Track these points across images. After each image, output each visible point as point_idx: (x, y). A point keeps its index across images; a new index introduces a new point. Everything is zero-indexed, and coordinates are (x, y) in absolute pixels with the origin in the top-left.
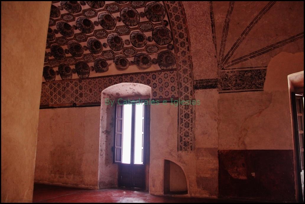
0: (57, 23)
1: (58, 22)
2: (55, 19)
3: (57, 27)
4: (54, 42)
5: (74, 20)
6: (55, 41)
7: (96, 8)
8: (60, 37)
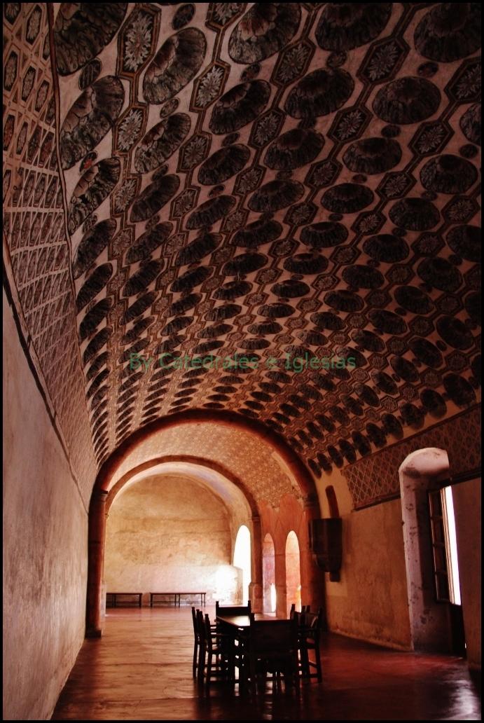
0: (447, 238)
1: (446, 233)
2: (435, 229)
3: (450, 247)
4: (464, 288)
6: (464, 285)
8: (471, 270)
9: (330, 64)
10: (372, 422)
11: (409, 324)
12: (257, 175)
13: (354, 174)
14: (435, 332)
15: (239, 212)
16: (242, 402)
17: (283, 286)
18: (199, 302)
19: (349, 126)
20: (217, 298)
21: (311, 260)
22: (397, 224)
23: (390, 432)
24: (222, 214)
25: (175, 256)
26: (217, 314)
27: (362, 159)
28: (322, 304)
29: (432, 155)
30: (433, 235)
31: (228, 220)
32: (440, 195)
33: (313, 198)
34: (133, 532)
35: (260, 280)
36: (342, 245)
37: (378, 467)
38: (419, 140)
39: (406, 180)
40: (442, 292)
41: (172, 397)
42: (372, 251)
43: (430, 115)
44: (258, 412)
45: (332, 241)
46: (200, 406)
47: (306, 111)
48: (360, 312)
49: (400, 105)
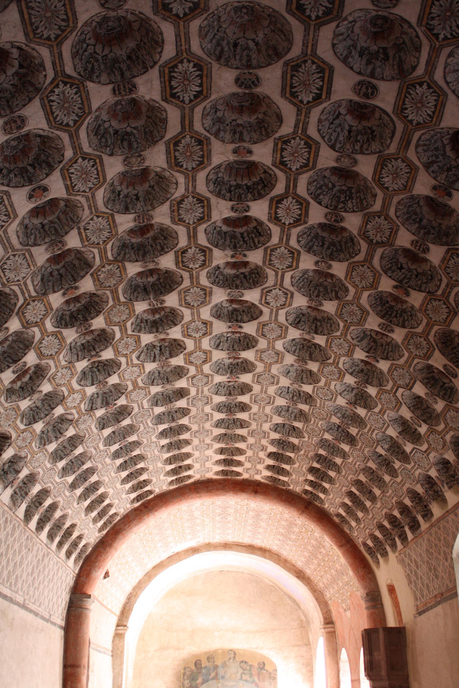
0: (397, 217)
3: (406, 228)
4: (447, 285)
5: (413, 170)
6: (445, 281)
7: (414, 68)
9: (106, 6)
10: (411, 486)
11: (403, 343)
12: (93, 166)
13: (233, 146)
14: (437, 353)
15: (98, 217)
16: (260, 467)
17: (230, 308)
18: (113, 339)
19: (186, 83)
20: (139, 331)
21: (248, 270)
22: (327, 207)
23: (433, 500)
24: (74, 222)
25: (29, 282)
26: (157, 352)
27: (238, 125)
28: (287, 328)
29: (321, 103)
30: (378, 215)
32: (359, 157)
33: (195, 187)
34: (179, 649)
35: (186, 303)
36: (269, 244)
37: (431, 550)
38: (292, 87)
39: (305, 144)
40: (424, 294)
41: (160, 465)
42: (315, 248)
43: (289, 50)
44: (286, 479)
45: (256, 240)
46: (210, 475)
47: (116, 73)
48: (338, 334)
49: (251, 44)
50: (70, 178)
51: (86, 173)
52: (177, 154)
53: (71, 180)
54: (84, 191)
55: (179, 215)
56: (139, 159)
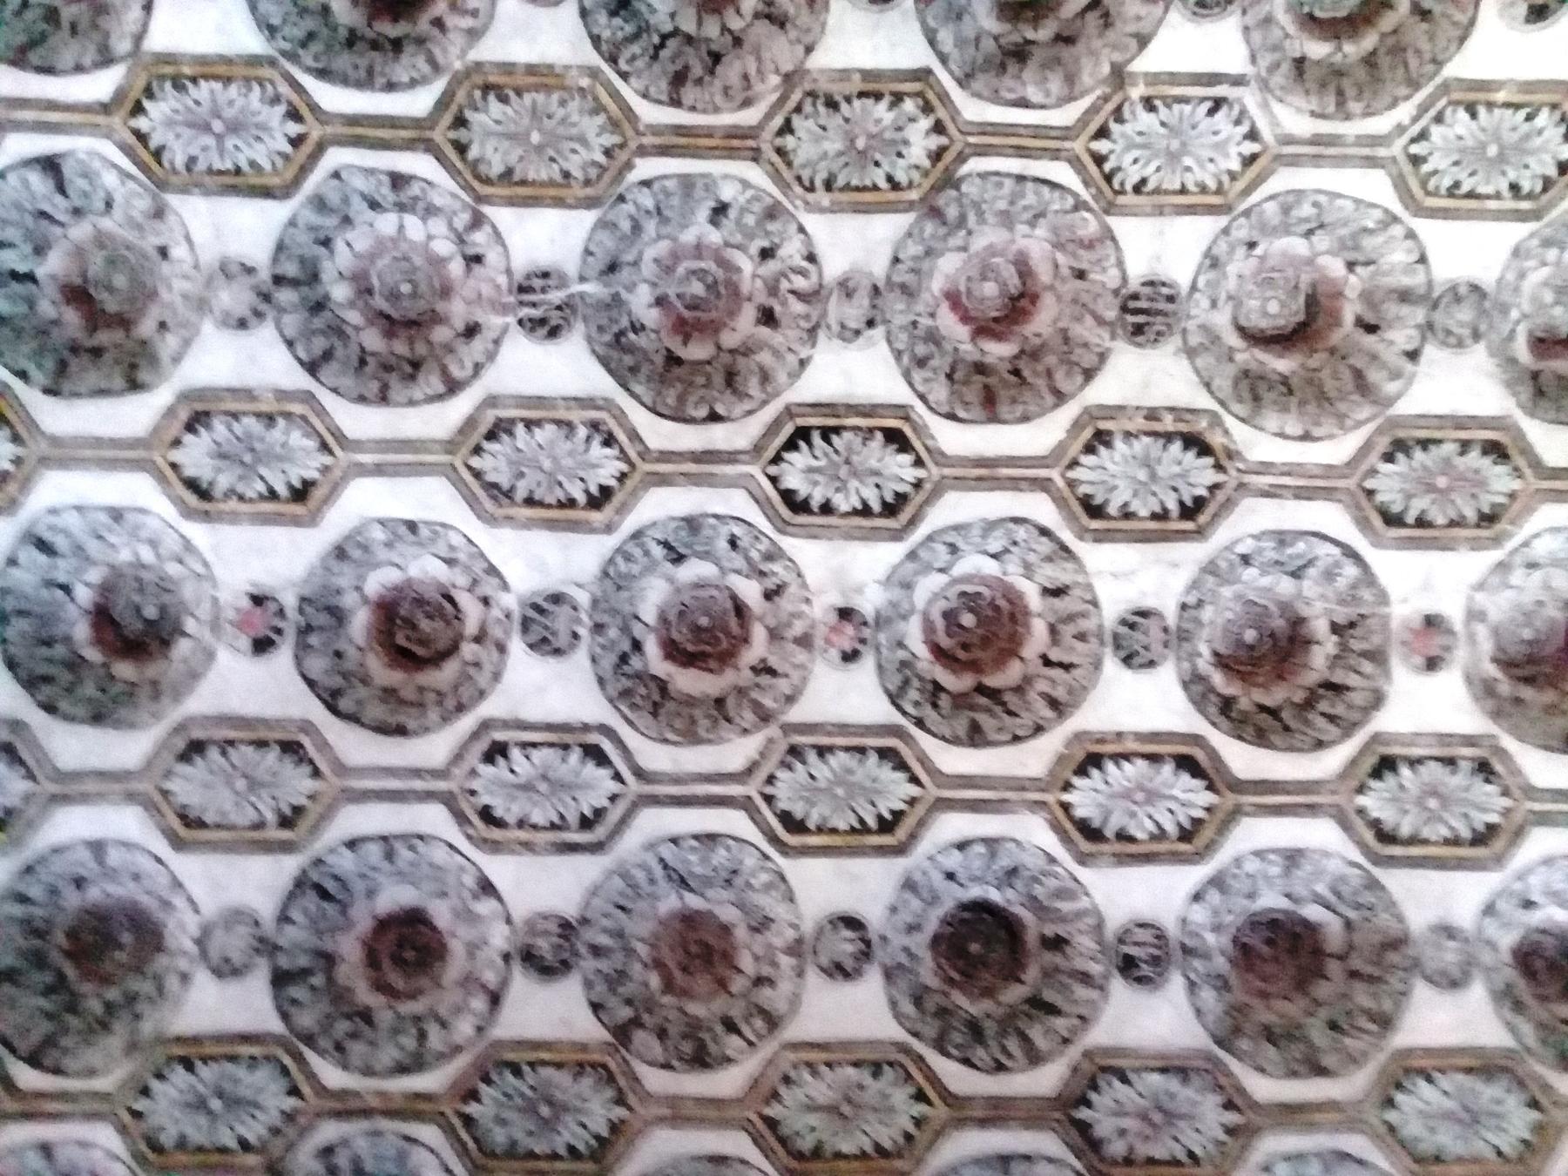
17: (349, 600)
31: (1218, 104)
50: (1517, 107)
51: (1502, 158)
52: (1449, 448)
53: (1507, 105)
54: (1423, 136)
55: (1128, 435)
56: (1466, 332)
